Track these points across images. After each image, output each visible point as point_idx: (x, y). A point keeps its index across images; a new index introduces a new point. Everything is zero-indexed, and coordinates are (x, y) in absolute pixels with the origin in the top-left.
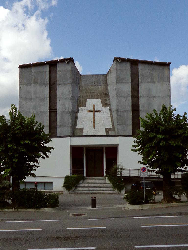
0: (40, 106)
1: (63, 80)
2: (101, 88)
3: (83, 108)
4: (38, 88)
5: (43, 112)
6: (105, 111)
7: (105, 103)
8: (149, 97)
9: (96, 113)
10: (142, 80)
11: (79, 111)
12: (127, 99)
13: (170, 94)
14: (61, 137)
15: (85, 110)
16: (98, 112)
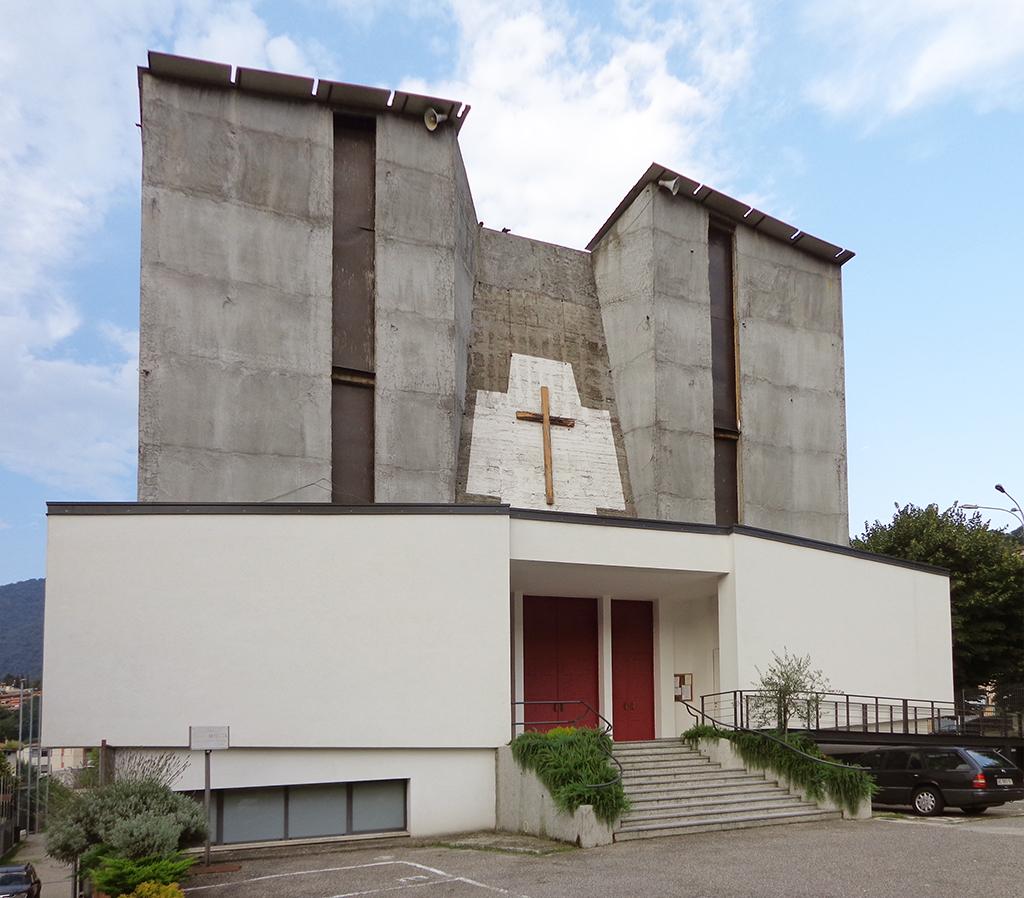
0: (282, 336)
1: (408, 218)
2: (573, 312)
3: (497, 394)
4: (269, 229)
5: (296, 376)
6: (595, 425)
7: (592, 388)
8: (776, 387)
9: (557, 432)
10: (749, 305)
11: (478, 409)
12: (697, 381)
13: (843, 386)
14: (451, 510)
15: (502, 407)
16: (565, 425)
